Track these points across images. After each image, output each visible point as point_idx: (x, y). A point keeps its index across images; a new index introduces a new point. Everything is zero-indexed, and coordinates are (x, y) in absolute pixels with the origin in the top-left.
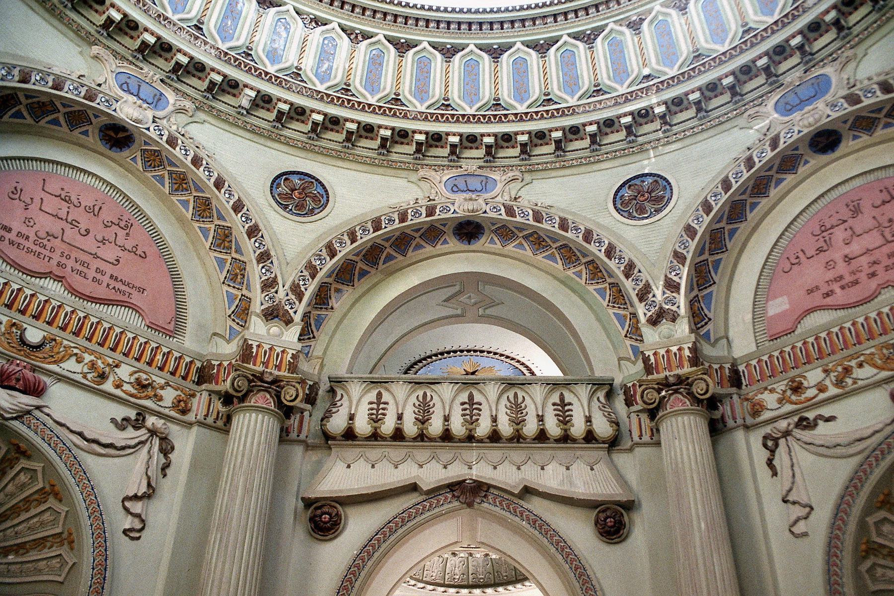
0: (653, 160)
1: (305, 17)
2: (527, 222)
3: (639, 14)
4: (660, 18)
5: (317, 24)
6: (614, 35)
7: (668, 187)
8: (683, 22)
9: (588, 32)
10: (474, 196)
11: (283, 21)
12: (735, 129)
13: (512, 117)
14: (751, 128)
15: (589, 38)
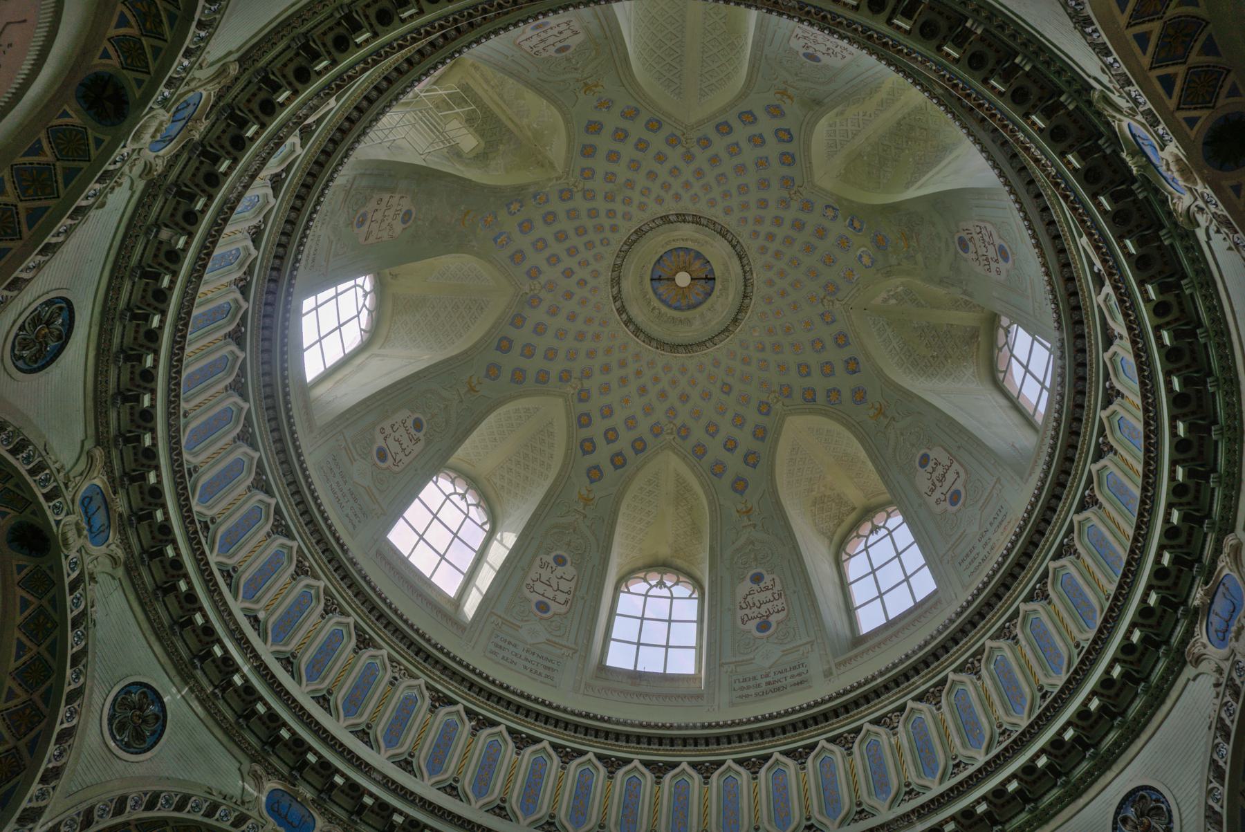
0: (179, 697)
2: (69, 611)
6: (285, 551)
7: (156, 736)
9: (283, 522)
10: (85, 532)
12: (237, 765)
13: (191, 529)
14: (243, 781)
15: (277, 527)
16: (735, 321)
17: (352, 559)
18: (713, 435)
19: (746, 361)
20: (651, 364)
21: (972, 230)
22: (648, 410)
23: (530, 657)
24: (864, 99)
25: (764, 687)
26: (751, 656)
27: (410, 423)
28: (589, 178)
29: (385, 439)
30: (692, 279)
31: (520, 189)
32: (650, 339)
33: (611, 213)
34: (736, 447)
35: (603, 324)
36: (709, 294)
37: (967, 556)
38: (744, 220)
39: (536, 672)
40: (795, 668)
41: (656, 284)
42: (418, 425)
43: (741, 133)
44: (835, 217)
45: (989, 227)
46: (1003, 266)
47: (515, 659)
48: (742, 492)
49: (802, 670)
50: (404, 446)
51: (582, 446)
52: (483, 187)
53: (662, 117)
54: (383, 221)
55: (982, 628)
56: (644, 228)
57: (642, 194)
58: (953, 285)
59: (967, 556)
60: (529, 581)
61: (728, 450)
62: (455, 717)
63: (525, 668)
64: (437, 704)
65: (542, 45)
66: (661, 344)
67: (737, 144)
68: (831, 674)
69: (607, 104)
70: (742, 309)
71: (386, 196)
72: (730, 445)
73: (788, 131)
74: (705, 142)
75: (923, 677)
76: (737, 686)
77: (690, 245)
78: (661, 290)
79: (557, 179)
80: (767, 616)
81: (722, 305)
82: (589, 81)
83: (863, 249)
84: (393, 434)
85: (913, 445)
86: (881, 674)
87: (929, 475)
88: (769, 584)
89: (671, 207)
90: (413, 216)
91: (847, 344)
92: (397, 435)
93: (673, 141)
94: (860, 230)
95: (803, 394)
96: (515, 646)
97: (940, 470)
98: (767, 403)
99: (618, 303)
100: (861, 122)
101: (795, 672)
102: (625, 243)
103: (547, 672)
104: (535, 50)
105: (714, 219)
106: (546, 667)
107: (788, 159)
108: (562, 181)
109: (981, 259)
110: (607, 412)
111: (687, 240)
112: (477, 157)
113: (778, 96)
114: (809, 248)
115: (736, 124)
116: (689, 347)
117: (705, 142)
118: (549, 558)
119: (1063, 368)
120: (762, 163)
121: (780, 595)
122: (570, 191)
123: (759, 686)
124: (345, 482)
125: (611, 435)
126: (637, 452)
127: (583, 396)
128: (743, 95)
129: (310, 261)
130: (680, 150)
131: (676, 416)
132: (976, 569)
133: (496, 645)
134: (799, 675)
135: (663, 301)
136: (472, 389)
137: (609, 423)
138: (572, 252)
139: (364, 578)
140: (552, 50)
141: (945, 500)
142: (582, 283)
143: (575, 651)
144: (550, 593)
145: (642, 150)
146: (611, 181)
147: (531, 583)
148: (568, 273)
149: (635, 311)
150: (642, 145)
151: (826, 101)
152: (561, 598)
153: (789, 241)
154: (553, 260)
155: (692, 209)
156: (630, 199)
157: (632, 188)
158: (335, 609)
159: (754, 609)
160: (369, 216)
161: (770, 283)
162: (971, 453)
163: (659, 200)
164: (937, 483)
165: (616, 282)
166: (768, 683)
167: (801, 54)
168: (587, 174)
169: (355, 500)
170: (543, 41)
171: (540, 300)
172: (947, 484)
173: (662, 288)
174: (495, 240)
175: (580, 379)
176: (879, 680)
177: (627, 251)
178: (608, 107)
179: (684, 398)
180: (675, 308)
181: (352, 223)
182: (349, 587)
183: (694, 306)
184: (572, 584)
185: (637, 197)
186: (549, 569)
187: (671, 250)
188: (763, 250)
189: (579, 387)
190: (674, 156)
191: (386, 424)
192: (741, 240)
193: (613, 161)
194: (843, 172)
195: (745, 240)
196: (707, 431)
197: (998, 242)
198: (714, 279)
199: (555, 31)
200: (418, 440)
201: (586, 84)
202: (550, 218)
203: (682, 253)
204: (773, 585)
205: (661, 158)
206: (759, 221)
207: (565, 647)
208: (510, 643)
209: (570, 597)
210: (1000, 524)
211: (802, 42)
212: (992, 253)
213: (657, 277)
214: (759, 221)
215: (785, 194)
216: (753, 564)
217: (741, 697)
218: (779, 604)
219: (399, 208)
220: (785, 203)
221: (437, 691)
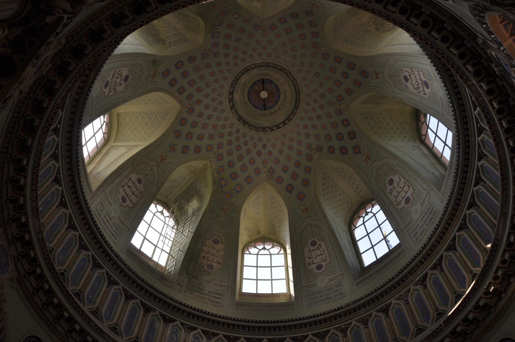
1: (185, 326)
3: (345, 325)
4: (355, 328)
5: (190, 329)
6: (334, 336)
8: (366, 332)
11: (175, 330)
16: (282, 70)
17: (346, 305)
23: (424, 220)
24: (157, 30)
27: (311, 248)
28: (212, 147)
29: (313, 263)
31: (215, 182)
32: (293, 113)
33: (230, 134)
35: (285, 135)
36: (271, 82)
38: (229, 71)
39: (431, 220)
42: (314, 243)
47: (423, 229)
50: (320, 254)
51: (343, 154)
52: (211, 201)
53: (179, 118)
54: (214, 255)
57: (220, 120)
60: (395, 203)
62: (433, 276)
63: (428, 224)
64: (425, 283)
66: (296, 107)
69: (173, 148)
70: (275, 67)
71: (203, 254)
74: (190, 97)
77: (246, 92)
79: (211, 162)
80: (422, 81)
81: (276, 76)
83: (230, 18)
84: (313, 259)
89: (226, 105)
90: (216, 238)
92: (314, 256)
96: (418, 225)
99: (274, 128)
100: (169, 28)
102: (245, 126)
103: (433, 213)
104: (139, 195)
105: (230, 84)
106: (430, 213)
108: (213, 162)
111: (243, 94)
112: (200, 200)
115: (177, 87)
116: (298, 93)
118: (389, 187)
120: (197, 69)
121: (412, 71)
122: (218, 155)
124: (322, 292)
125: (340, 137)
126: (349, 124)
127: (320, 149)
129: (218, 296)
133: (415, 236)
136: (306, 210)
138: (248, 152)
139: (356, 301)
142: (264, 146)
143: (428, 192)
144: (403, 194)
145: (197, 125)
146: (214, 136)
147: (397, 202)
148: (259, 153)
149: (279, 118)
150: (194, 125)
152: (406, 188)
153: (236, 49)
154: (252, 161)
156: (222, 126)
158: (367, 319)
160: (209, 262)
161: (260, 54)
163: (223, 111)
165: (264, 129)
167: (126, 83)
168: (209, 148)
169: (331, 289)
170: (133, 193)
171: (271, 168)
174: (238, 192)
177: (249, 125)
179: (323, 96)
180: (279, 97)
181: (210, 272)
182: (360, 310)
183: (278, 88)
184: (402, 179)
186: (393, 189)
187: (250, 101)
188: (243, 60)
189: (315, 151)
191: (308, 261)
192: (240, 71)
193: (203, 137)
198: (263, 79)
199: (128, 190)
200: (320, 245)
201: (161, 161)
202: (231, 164)
207: (425, 198)
208: (416, 228)
209: (407, 183)
211: (117, 88)
213: (263, 107)
214: (228, 64)
219: (210, 246)
221: (419, 280)
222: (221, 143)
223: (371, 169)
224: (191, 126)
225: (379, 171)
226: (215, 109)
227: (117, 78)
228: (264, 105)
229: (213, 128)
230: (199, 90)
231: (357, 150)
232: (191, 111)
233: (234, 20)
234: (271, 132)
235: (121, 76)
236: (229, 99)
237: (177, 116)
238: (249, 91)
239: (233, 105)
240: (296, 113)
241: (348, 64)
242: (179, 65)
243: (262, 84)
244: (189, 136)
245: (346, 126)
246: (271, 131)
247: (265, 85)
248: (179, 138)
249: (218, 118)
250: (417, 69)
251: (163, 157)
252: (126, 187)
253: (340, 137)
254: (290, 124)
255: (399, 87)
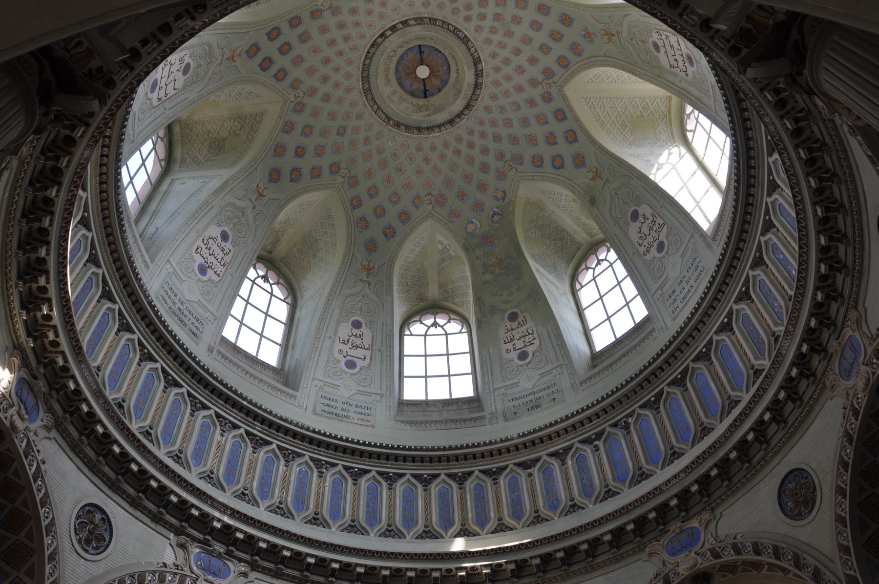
16: (398, 125)
18: (303, 133)
19: (367, 141)
20: (350, 62)
21: (528, 326)
22: (311, 71)
25: (175, 308)
26: (184, 278)
28: (517, 4)
30: (424, 79)
32: (369, 56)
34: (300, 157)
35: (382, 16)
36: (412, 94)
37: (329, 399)
38: (481, 123)
40: (197, 320)
41: (417, 50)
43: (558, 129)
44: (497, 199)
45: (537, 342)
46: (514, 355)
48: (270, 181)
49: (199, 326)
51: (273, 29)
55: (313, 449)
56: (470, 43)
57: (500, 43)
58: (480, 309)
59: (329, 399)
61: (296, 151)
65: (667, 42)
66: (366, 68)
67: (547, 122)
68: (212, 352)
70: (408, 128)
72: (300, 152)
73: (562, 166)
74: (547, 98)
75: (263, 428)
76: (166, 288)
77: (453, 75)
78: (410, 54)
82: (615, 38)
83: (479, 226)
85: (361, 310)
86: (250, 402)
87: (350, 334)
88: (227, 250)
89: (487, 65)
91: (403, 222)
93: (548, 73)
94: (492, 221)
95: (355, 197)
97: (358, 341)
98: (339, 169)
101: (197, 324)
102: (456, 28)
107: (538, 161)
109: (509, 333)
110: (304, 38)
111: (458, 73)
113: (594, 170)
114: (468, 178)
116: (368, 92)
117: (547, 98)
118: (187, 60)
119: (496, 442)
121: (224, 265)
123: (175, 303)
128: (594, 142)
130: (540, 77)
131: (311, 95)
132: (328, 413)
134: (197, 328)
135: (402, 57)
137: (295, 42)
140: (660, 43)
141: (345, 357)
146: (513, 20)
149: (394, 40)
151: (595, 209)
153: (470, 160)
155: (486, 80)
157: (505, 35)
159: (207, 251)
161: (433, 148)
162: (382, 362)
163: (494, 55)
164: (350, 343)
166: (179, 309)
167: (637, 208)
172: (353, 352)
173: (414, 55)
175: (330, 7)
176: (245, 403)
178: (584, 36)
179: (326, 98)
180: (397, 68)
183: (401, 84)
185: (497, 38)
187: (447, 59)
188: (459, 139)
189: (324, 8)
190: (535, 72)
194: (531, 200)
195: (464, 124)
196: (304, 128)
197: (530, 349)
198: (426, 97)
199: (679, 58)
203: (445, 68)
204: (227, 254)
205: (533, 61)
206: (483, 135)
210: (361, 414)
212: (519, 344)
213: (423, 49)
214: (483, 135)
215: (508, 157)
216: (231, 226)
217: (163, 298)
218: (220, 269)
220: (501, 156)
222: (499, 5)
223: (222, 49)
224: (551, 49)
225: (209, 61)
226: (507, 61)
227: (645, 236)
228: (422, 54)
229: (513, 33)
230: (532, 103)
231: (253, 51)
232: (548, 73)
233: (475, 221)
234: (407, 18)
235: (640, 232)
236: (482, 75)
237: (573, 75)
238: (449, 76)
239: (475, 64)
240: (366, 58)
241: (301, 175)
242: (558, 163)
243: (427, 88)
244: (556, 36)
245: (278, 71)
246: (407, 20)
247: (422, 87)
248: (575, 43)
249: (503, 46)
250: (223, 277)
251: (607, 37)
252: (681, 64)
253: (285, 49)
254: (374, 36)
255: (228, 208)
